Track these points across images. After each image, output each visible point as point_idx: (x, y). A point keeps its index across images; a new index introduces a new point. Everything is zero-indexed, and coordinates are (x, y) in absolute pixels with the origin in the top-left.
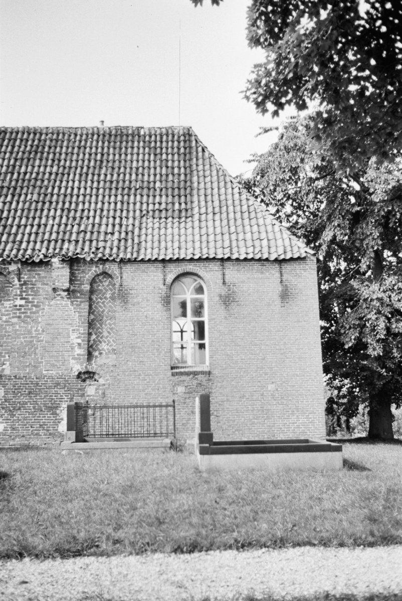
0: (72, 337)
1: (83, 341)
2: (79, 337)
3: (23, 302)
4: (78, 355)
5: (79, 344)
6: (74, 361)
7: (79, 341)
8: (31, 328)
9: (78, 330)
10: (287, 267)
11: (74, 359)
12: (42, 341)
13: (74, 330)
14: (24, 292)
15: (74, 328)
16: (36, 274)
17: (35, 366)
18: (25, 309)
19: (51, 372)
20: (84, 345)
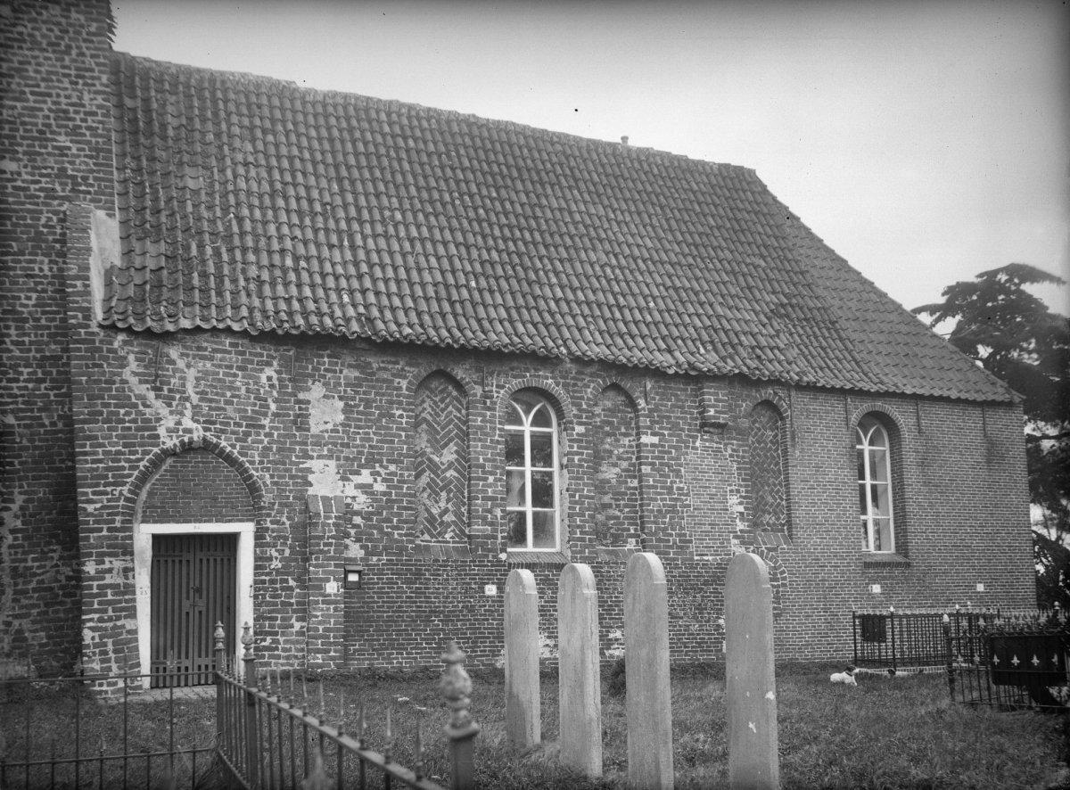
0: (730, 502)
1: (746, 508)
2: (741, 503)
3: (655, 440)
4: (741, 531)
5: (742, 514)
6: (736, 541)
7: (741, 509)
8: (671, 482)
9: (738, 491)
10: (926, 408)
11: (736, 537)
12: (689, 506)
13: (731, 491)
14: (657, 423)
15: (733, 487)
16: (672, 394)
17: (681, 547)
18: (659, 452)
19: (706, 558)
20: (748, 515)
